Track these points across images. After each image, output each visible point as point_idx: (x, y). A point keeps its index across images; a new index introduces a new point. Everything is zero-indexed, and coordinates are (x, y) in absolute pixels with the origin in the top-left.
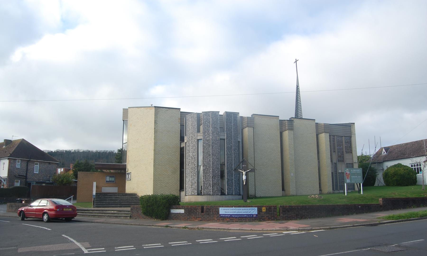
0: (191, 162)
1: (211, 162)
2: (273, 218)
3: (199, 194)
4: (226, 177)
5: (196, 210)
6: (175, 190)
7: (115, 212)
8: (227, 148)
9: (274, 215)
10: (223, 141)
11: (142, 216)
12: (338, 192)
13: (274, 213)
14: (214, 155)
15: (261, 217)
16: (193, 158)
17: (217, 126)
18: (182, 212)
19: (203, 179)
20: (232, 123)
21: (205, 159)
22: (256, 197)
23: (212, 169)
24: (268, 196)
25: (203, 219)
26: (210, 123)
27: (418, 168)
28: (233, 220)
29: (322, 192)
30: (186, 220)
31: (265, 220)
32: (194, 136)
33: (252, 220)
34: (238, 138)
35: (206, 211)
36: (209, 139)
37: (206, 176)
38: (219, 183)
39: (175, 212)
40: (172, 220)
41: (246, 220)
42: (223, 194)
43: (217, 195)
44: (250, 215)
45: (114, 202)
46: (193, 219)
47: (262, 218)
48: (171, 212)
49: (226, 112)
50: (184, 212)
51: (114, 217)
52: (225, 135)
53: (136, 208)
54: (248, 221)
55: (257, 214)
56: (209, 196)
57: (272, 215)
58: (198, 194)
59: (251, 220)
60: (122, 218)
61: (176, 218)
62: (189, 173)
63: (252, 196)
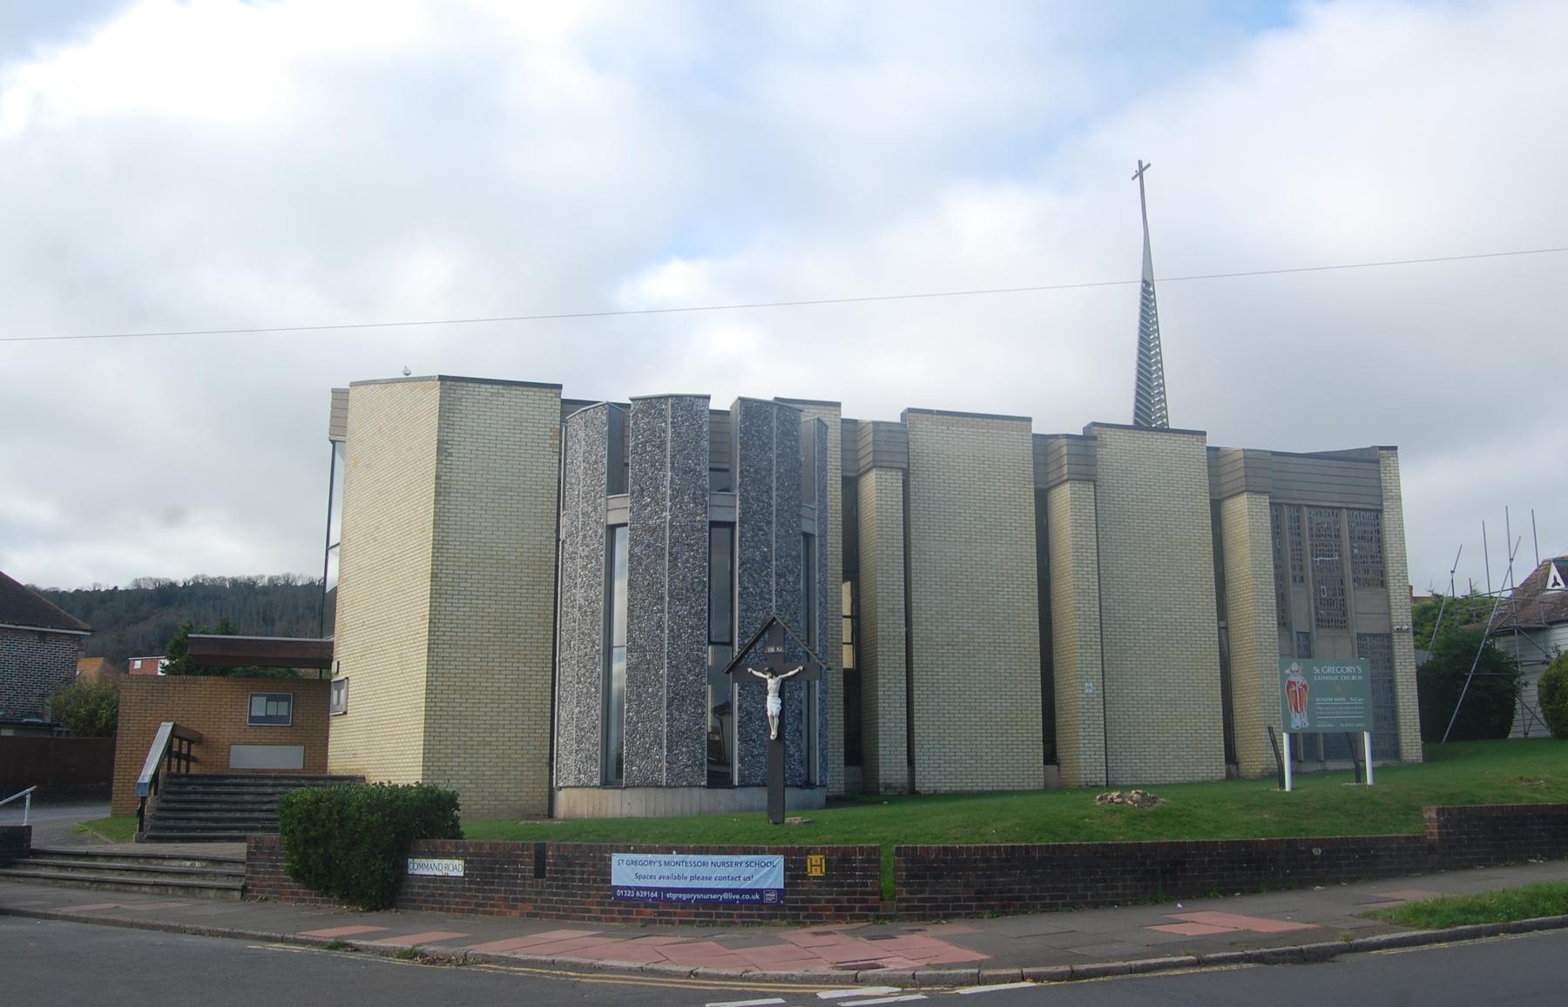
0: (577, 631)
1: (667, 632)
2: (861, 909)
4: (737, 703)
5: (515, 863)
7: (197, 864)
8: (741, 565)
9: (862, 893)
10: (727, 531)
11: (289, 887)
12: (1319, 767)
13: (865, 885)
14: (679, 600)
15: (803, 901)
16: (586, 611)
18: (455, 873)
19: (628, 712)
20: (770, 449)
22: (918, 793)
24: (976, 789)
25: (542, 908)
28: (669, 914)
29: (1238, 769)
31: (820, 917)
32: (595, 509)
33: (760, 916)
34: (799, 516)
36: (659, 525)
37: (639, 696)
41: (730, 916)
42: (719, 780)
43: (690, 786)
44: (751, 891)
45: (247, 815)
46: (499, 907)
47: (806, 909)
48: (410, 872)
49: (743, 401)
50: (462, 874)
51: (180, 892)
52: (735, 507)
54: (737, 920)
55: (782, 887)
56: (652, 791)
57: (855, 893)
58: (606, 784)
59: (751, 916)
60: (211, 893)
62: (570, 682)
63: (895, 788)
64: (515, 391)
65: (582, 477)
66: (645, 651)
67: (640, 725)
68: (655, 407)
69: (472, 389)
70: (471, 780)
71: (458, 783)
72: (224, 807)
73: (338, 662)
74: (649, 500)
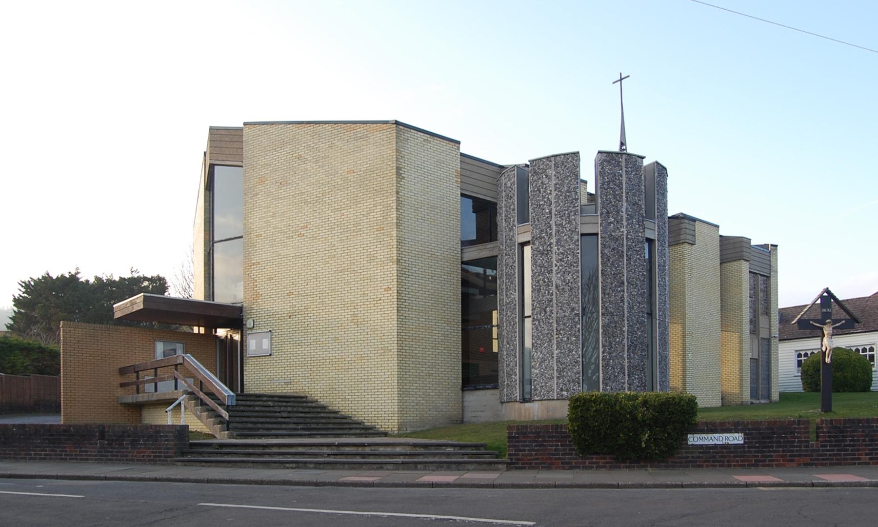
5: (791, 433)
6: (452, 387)
16: (563, 289)
17: (640, 200)
18: (736, 442)
19: (603, 352)
21: (608, 294)
25: (816, 460)
30: (748, 465)
35: (829, 437)
37: (611, 343)
38: (644, 364)
39: (706, 442)
46: (779, 461)
48: (689, 443)
50: (742, 442)
53: (532, 433)
61: (709, 461)
66: (613, 315)
67: (611, 361)
70: (423, 398)
71: (416, 400)
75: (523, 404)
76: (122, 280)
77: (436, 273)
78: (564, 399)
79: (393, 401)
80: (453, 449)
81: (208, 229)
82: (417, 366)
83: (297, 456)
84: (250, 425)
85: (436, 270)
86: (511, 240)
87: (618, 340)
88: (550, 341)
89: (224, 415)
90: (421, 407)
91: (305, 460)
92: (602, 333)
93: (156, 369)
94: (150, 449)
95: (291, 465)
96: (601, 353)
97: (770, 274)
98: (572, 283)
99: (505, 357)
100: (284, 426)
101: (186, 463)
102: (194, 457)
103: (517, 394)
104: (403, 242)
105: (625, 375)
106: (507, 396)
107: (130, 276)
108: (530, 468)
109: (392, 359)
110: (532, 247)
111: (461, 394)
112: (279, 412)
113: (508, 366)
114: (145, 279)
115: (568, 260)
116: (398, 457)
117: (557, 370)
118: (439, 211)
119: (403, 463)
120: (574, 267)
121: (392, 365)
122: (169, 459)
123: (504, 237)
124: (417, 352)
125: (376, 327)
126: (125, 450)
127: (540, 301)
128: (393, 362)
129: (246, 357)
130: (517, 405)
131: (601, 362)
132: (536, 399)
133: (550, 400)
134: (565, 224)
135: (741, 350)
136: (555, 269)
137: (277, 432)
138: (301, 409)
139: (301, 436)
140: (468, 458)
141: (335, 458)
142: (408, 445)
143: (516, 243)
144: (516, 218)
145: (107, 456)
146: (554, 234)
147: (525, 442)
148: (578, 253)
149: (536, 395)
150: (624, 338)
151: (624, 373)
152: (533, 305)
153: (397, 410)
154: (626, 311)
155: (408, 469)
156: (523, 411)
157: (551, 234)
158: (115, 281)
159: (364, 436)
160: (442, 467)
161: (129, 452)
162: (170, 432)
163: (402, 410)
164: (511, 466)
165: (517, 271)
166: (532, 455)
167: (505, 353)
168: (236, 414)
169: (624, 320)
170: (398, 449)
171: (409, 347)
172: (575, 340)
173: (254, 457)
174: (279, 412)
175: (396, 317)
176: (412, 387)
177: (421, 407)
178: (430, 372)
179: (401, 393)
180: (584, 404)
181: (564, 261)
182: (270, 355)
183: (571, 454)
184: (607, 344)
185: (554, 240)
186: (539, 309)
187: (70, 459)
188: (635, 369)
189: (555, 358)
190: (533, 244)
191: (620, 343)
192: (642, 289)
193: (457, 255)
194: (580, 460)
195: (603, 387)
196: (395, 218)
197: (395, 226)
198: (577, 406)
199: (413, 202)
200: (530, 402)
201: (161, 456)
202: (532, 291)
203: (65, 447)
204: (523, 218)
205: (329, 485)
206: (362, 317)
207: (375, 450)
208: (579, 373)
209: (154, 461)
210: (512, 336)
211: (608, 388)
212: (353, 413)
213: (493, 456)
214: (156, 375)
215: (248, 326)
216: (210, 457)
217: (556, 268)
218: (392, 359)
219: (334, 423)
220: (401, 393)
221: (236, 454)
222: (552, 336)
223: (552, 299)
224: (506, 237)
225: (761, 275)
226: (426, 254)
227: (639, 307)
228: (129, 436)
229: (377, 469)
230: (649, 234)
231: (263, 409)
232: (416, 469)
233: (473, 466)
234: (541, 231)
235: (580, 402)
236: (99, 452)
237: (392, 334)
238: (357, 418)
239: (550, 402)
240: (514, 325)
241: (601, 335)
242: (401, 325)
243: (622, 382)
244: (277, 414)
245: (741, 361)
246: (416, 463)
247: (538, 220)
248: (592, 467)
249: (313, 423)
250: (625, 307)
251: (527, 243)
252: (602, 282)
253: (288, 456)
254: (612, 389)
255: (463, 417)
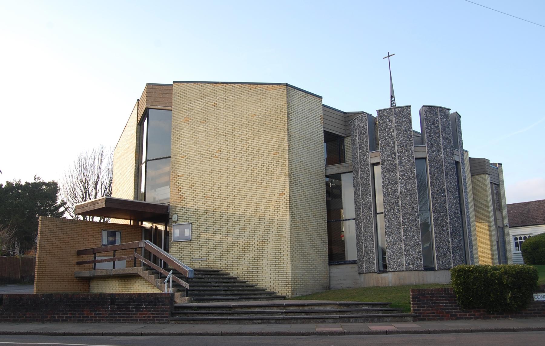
3: (428, 268)
11: (448, 312)
14: (450, 192)
16: (406, 194)
19: (436, 238)
23: (451, 219)
26: (439, 129)
27: (518, 242)
38: (461, 246)
40: (539, 316)
48: (535, 300)
53: (429, 294)
64: (309, 96)
65: (395, 136)
68: (433, 111)
69: (296, 92)
72: (205, 284)
73: (178, 216)
74: (435, 149)
75: (380, 275)
76: (27, 184)
77: (312, 183)
78: (411, 271)
79: (287, 273)
80: (367, 307)
81: (138, 151)
82: (302, 248)
83: (258, 315)
84: (197, 292)
85: (311, 181)
86: (365, 161)
87: (444, 229)
88: (399, 230)
89: (184, 285)
90: (305, 277)
91: (269, 317)
92: (434, 224)
93: (115, 251)
94: (150, 311)
95: (258, 321)
96: (434, 238)
97: (499, 183)
98: (411, 190)
99: (363, 241)
100: (218, 292)
101: (178, 322)
102: (181, 317)
103: (375, 268)
104: (292, 162)
105: (450, 253)
106: (366, 269)
107: (33, 181)
108: (429, 320)
109: (286, 243)
110: (381, 167)
111: (328, 268)
112: (210, 282)
113: (366, 247)
114: (44, 183)
115: (408, 175)
116: (332, 313)
117: (405, 250)
118: (312, 142)
119: (340, 318)
120: (412, 180)
121: (287, 247)
122: (165, 319)
123: (359, 160)
124: (302, 238)
125: (273, 220)
126: (130, 313)
127: (390, 202)
128: (287, 245)
129: (171, 242)
130: (375, 275)
131: (435, 244)
132: (390, 270)
133: (401, 271)
134: (404, 152)
135: (490, 235)
136: (399, 181)
137: (218, 297)
138: (221, 280)
139: (233, 300)
140: (383, 313)
141: (287, 315)
142: (336, 304)
143: (370, 164)
144: (369, 147)
145: (116, 317)
146: (397, 158)
147: (424, 300)
148: (415, 171)
149: (390, 268)
150: (448, 228)
151: (450, 252)
152: (384, 205)
153: (290, 279)
154: (448, 209)
155: (343, 322)
156: (380, 280)
157: (395, 158)
158: (21, 185)
159: (271, 299)
160: (368, 320)
161: (134, 314)
162: (166, 298)
163: (294, 279)
164: (416, 318)
165: (371, 182)
166: (429, 310)
167: (363, 238)
168: (192, 284)
169: (447, 215)
170: (328, 308)
171: (297, 234)
172: (416, 229)
173: (226, 316)
174: (210, 282)
175: (289, 213)
176: (299, 263)
177: (305, 277)
178: (310, 252)
179: (293, 267)
180: (465, 274)
181: (405, 176)
182: (191, 240)
183: (456, 309)
184: (438, 232)
185: (397, 162)
186: (389, 208)
187: (86, 320)
188: (456, 249)
189: (403, 242)
190: (383, 164)
191: (446, 231)
192: (456, 195)
193: (323, 171)
194: (463, 313)
195: (437, 262)
196: (287, 146)
197: (287, 152)
198: (460, 275)
199: (297, 136)
200: (386, 273)
201: (158, 317)
202: (383, 196)
203: (83, 312)
204: (374, 146)
205: (312, 335)
206: (263, 214)
207: (311, 309)
208: (420, 252)
209: (152, 321)
210: (368, 226)
211: (441, 262)
212: (256, 282)
213: (399, 311)
214: (114, 256)
215: (173, 219)
216: (192, 316)
217: (400, 180)
218: (286, 243)
219: (248, 290)
220: (293, 267)
221: (212, 313)
222: (400, 227)
223: (398, 201)
224: (360, 159)
225: (494, 184)
226: (305, 170)
227: (455, 207)
228: (134, 302)
229: (321, 322)
230: (457, 159)
231: (198, 280)
232: (349, 322)
233: (390, 319)
234: (388, 156)
235: (462, 272)
236: (110, 314)
237: (286, 225)
238: (259, 286)
239: (401, 273)
240: (370, 218)
241: (433, 226)
242: (292, 219)
243: (449, 258)
244: (209, 284)
245: (491, 243)
246: (349, 318)
247: (385, 148)
248: (471, 318)
249: (235, 290)
250: (447, 207)
251: (377, 164)
252: (431, 190)
253: (252, 315)
254: (443, 263)
255: (330, 285)
